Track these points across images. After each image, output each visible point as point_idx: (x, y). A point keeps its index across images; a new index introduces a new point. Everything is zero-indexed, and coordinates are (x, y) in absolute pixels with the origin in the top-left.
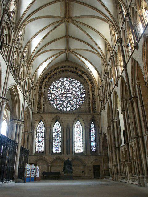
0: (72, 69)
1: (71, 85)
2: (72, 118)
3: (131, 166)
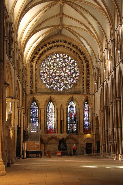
0: (65, 44)
2: (66, 98)
3: (114, 146)
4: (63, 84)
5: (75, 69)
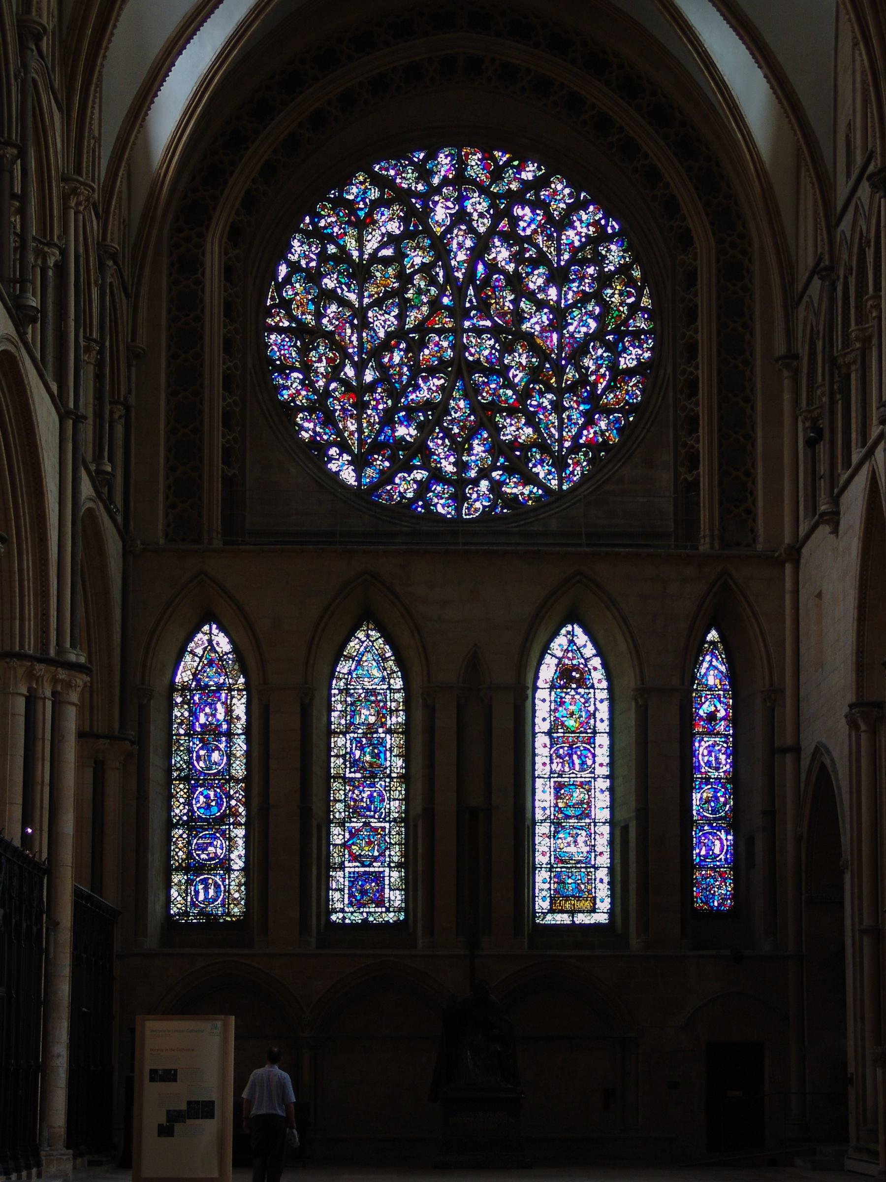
1: (511, 238)
5: (606, 307)
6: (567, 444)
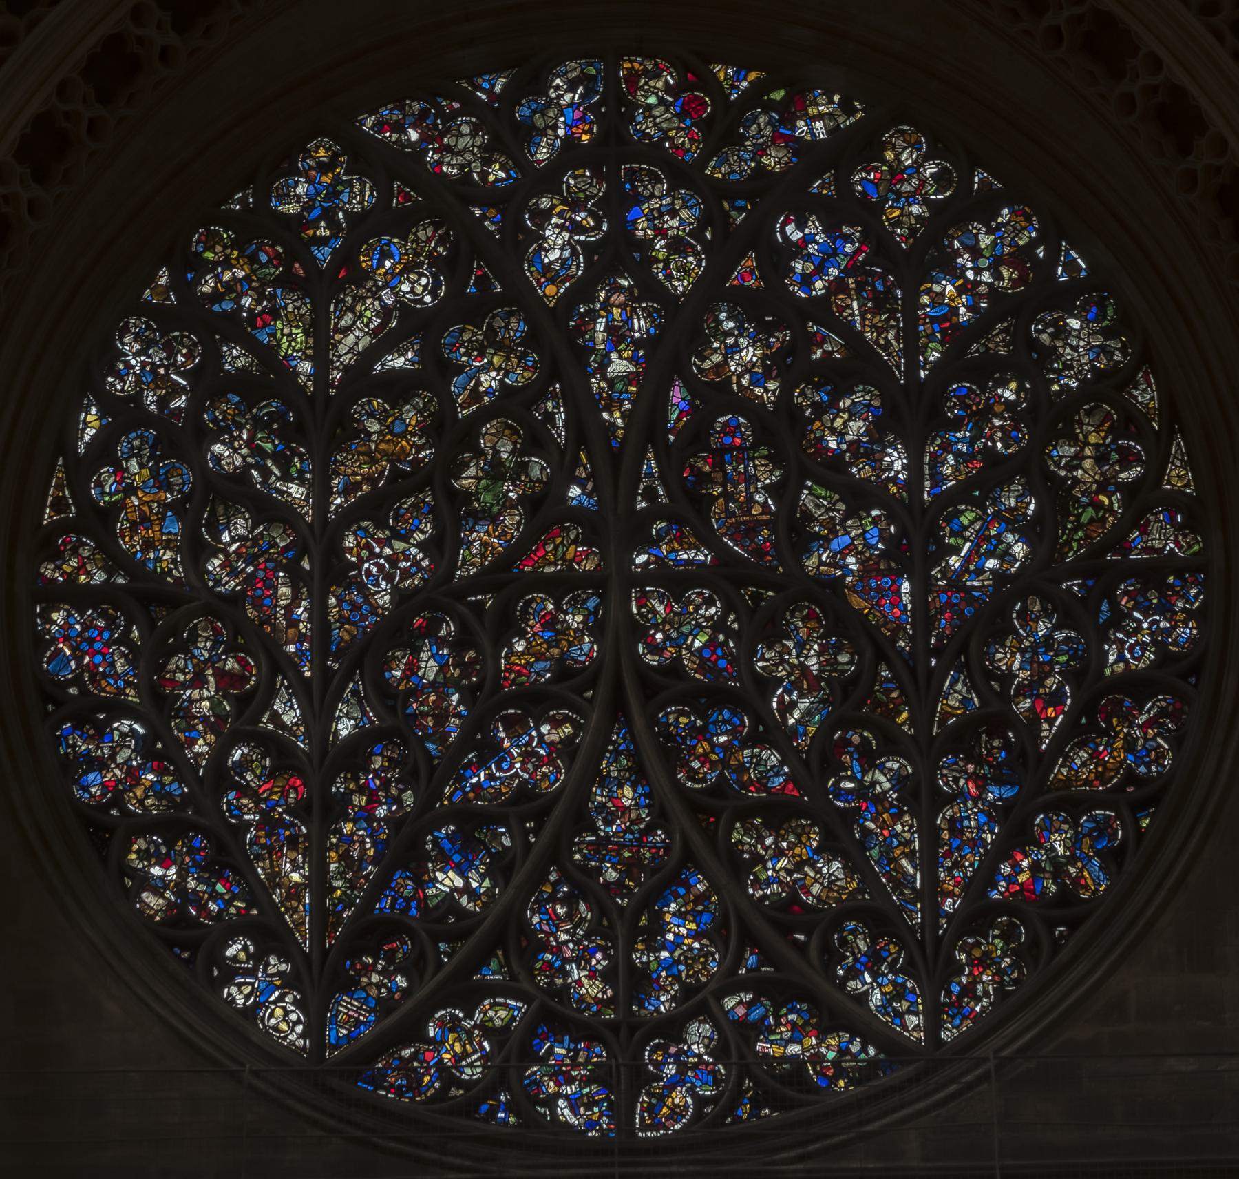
4: (714, 933)
6: (948, 905)
